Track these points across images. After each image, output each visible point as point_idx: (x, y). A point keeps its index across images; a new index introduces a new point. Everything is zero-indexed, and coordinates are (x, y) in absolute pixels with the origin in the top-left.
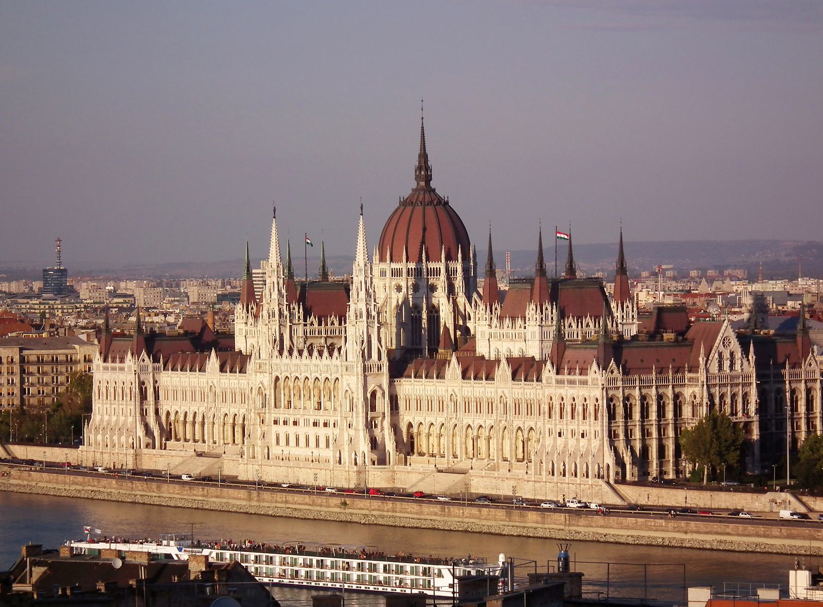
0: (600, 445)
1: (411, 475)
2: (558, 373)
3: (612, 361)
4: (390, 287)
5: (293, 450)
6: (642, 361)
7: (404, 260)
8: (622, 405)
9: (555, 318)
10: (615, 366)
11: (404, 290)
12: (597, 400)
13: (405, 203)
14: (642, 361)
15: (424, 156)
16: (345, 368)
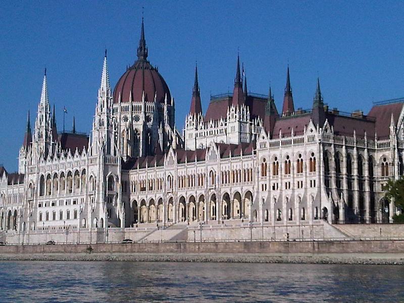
0: (318, 192)
1: (137, 234)
2: (271, 138)
3: (326, 121)
4: (120, 119)
5: (51, 223)
6: (344, 128)
7: (130, 101)
8: (333, 159)
9: (248, 118)
10: (328, 126)
11: (130, 119)
12: (313, 154)
13: (130, 69)
14: (344, 128)
15: (143, 42)
16: (90, 161)
